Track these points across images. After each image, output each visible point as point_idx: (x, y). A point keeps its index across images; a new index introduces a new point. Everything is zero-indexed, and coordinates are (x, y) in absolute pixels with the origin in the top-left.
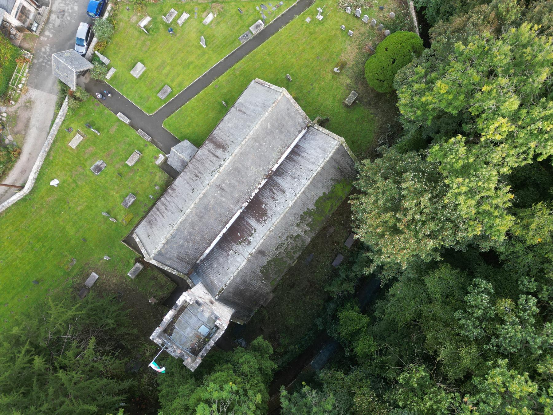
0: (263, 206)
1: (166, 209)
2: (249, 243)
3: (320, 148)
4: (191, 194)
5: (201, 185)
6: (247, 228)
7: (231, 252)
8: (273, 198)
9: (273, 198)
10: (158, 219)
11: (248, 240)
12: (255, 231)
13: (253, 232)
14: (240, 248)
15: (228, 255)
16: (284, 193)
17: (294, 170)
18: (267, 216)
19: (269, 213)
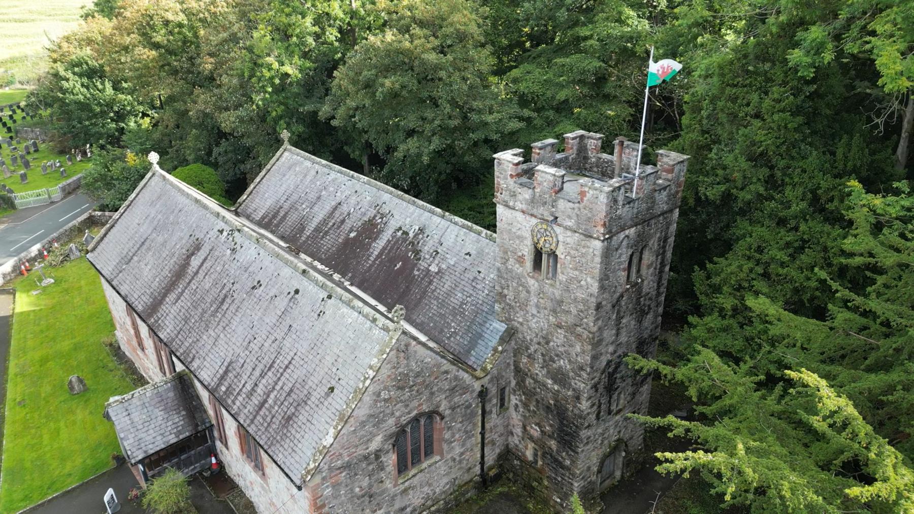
0: (352, 235)
1: (269, 369)
2: (421, 230)
3: (284, 176)
4: (262, 288)
5: (251, 269)
6: (390, 251)
7: (434, 269)
8: (343, 222)
9: (343, 222)
10: (287, 389)
11: (415, 236)
12: (400, 228)
13: (399, 234)
14: (427, 249)
15: (439, 271)
16: (340, 204)
17: (304, 206)
18: (375, 216)
19: (372, 212)
